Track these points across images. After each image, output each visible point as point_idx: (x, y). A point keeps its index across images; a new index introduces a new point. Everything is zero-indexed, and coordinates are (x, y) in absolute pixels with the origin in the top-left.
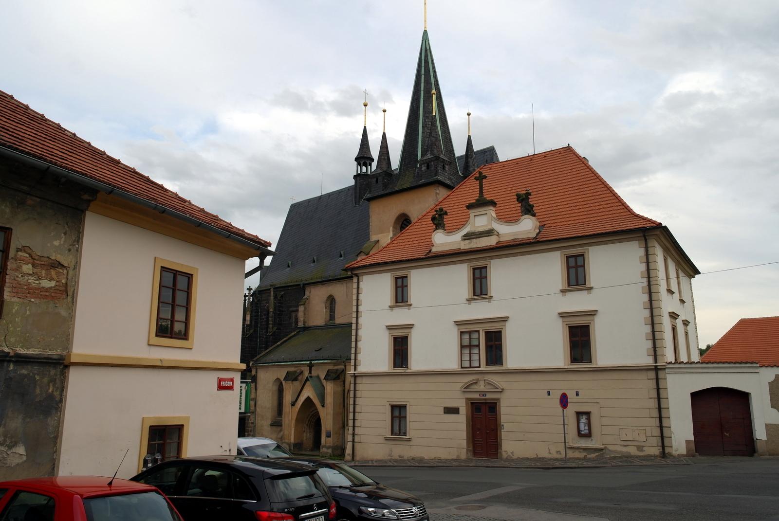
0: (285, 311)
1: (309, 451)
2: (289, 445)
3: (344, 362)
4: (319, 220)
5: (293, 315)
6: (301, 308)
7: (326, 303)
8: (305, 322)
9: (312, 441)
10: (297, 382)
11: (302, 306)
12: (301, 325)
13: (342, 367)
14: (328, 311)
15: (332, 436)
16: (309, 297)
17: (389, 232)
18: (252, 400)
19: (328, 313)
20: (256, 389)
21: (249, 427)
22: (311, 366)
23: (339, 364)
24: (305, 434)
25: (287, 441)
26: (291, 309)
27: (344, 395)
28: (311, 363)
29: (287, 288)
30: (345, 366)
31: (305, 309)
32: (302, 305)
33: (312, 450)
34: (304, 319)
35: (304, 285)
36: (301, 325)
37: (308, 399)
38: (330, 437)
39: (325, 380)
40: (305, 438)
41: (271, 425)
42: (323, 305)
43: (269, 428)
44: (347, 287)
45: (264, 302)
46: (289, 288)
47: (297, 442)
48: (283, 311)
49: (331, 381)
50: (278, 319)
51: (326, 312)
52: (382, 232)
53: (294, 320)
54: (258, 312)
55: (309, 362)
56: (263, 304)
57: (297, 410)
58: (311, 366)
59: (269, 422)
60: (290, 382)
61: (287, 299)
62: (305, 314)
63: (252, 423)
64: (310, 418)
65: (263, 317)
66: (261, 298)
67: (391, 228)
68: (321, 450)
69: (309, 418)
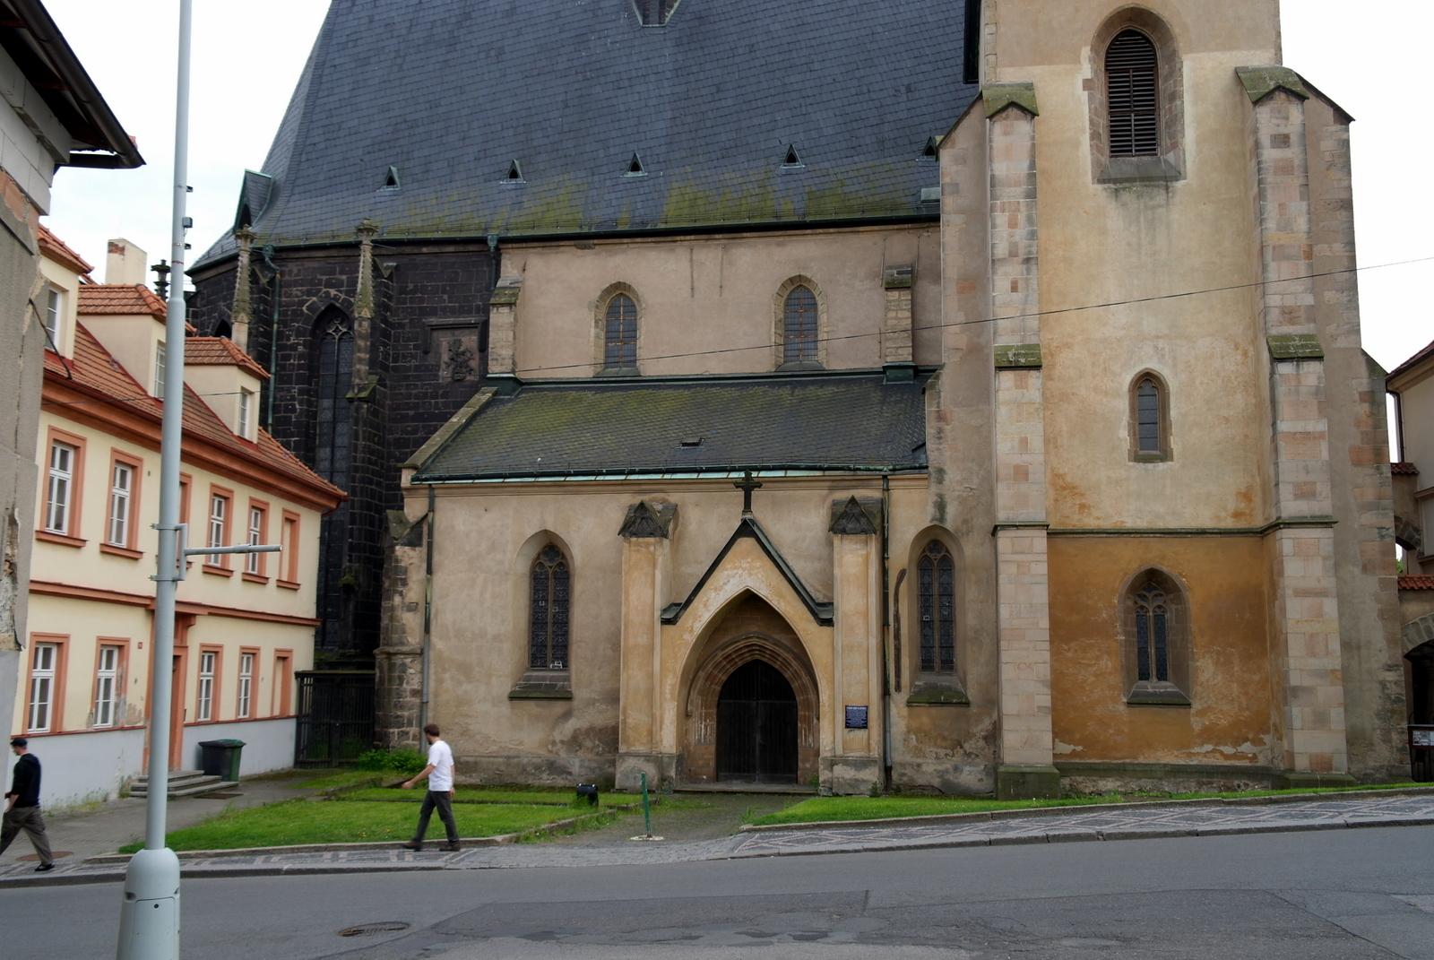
0: (401, 326)
1: (708, 781)
2: (657, 760)
3: (885, 477)
4: (493, 53)
6: (500, 319)
9: (713, 748)
11: (505, 310)
14: (603, 334)
17: (1077, 61)
18: (412, 608)
19: (602, 342)
20: (429, 571)
21: (402, 707)
22: (748, 487)
23: (863, 483)
25: (641, 748)
26: (434, 320)
28: (748, 477)
29: (408, 250)
32: (502, 305)
33: (717, 779)
35: (503, 241)
36: (496, 369)
37: (748, 603)
38: (865, 726)
41: (513, 697)
42: (590, 317)
43: (505, 708)
44: (691, 260)
45: (295, 291)
46: (425, 250)
49: (863, 537)
50: (382, 349)
51: (597, 336)
52: (1046, 59)
53: (445, 357)
54: (270, 324)
55: (742, 475)
56: (290, 296)
58: (748, 487)
59: (506, 687)
60: (652, 540)
61: (411, 286)
63: (415, 693)
65: (293, 340)
66: (282, 274)
67: (1086, 52)
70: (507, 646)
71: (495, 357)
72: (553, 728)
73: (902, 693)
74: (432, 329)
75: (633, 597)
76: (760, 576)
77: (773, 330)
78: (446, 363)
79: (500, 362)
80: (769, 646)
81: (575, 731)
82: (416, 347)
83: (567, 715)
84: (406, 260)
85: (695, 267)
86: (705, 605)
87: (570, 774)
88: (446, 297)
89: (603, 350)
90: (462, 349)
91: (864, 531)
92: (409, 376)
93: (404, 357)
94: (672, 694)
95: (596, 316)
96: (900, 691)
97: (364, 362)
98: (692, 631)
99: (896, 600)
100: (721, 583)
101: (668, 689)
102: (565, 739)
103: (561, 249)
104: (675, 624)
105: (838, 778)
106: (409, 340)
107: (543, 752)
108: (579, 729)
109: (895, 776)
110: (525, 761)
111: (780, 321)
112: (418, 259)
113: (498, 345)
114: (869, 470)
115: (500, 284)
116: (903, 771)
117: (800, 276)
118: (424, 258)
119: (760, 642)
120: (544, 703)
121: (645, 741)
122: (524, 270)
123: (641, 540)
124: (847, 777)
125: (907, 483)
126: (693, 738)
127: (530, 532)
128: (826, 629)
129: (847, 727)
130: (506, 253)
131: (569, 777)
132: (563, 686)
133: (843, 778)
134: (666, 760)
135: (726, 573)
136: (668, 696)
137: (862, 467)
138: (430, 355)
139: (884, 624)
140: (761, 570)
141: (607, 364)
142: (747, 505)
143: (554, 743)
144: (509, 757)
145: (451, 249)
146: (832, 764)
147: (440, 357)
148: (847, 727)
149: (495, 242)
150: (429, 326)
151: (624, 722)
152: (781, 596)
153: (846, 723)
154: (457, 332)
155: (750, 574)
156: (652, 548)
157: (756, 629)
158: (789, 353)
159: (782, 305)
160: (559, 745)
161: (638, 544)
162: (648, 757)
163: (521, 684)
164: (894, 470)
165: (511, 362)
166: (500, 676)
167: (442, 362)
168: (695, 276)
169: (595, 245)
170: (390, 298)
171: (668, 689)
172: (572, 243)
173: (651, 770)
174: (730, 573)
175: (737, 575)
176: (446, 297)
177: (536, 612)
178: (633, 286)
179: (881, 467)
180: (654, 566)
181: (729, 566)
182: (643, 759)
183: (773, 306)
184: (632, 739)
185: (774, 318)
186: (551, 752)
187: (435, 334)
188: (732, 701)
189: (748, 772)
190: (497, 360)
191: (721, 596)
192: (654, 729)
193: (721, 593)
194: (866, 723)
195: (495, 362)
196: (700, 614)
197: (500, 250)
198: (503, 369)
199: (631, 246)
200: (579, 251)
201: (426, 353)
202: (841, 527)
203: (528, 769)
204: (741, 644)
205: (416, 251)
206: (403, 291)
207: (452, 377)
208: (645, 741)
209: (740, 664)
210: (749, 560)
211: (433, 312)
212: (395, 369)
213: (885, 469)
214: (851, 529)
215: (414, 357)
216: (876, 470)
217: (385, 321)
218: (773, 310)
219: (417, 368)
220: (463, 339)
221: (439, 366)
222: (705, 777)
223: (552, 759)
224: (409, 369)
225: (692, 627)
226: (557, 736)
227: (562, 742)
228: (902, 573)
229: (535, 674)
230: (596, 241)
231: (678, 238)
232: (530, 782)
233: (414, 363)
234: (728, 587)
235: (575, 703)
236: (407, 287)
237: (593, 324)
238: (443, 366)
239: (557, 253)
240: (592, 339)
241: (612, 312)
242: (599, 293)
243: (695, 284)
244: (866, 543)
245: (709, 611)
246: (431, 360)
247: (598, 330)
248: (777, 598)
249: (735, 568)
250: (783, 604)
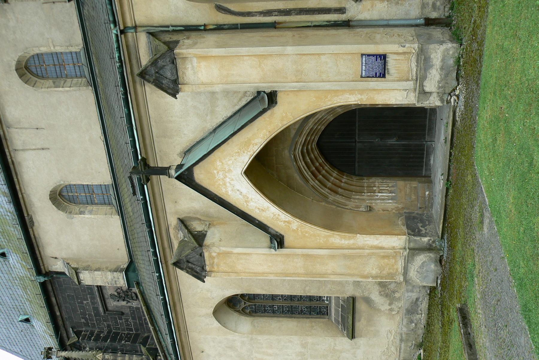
0: (109, 326)
1: (431, 189)
2: (414, 251)
3: (122, 32)
5: (112, 304)
7: (70, 213)
8: (117, 270)
9: (401, 183)
10: (209, 234)
11: (81, 276)
12: (122, 282)
13: (143, 40)
14: (90, 208)
15: (380, 49)
16: (64, 260)
19: (95, 208)
24: (378, 205)
25: (400, 265)
26: (101, 309)
27: (234, 27)
30: (135, 27)
31: (87, 268)
33: (428, 179)
34: (110, 271)
35: (39, 272)
38: (383, 57)
39: (177, 92)
40: (391, 205)
41: (353, 336)
43: (360, 341)
44: (23, 150)
47: (404, 229)
48: (109, 332)
49: (179, 61)
50: (123, 342)
51: (91, 212)
53: (124, 303)
57: (296, 223)
59: (343, 342)
60: (206, 255)
61: (83, 320)
62: (98, 269)
64: (326, 186)
68: (434, 102)
69: (325, 191)
70: (310, 340)
71: (114, 282)
72: (379, 310)
73: (347, 6)
74: (107, 310)
75: (260, 269)
76: (230, 162)
77: (61, 89)
78: (127, 303)
79: (117, 280)
80: (302, 139)
81: (381, 295)
82: (121, 319)
83: (368, 301)
84: (67, 323)
85: (28, 148)
86: (263, 210)
87: (417, 299)
88: (85, 302)
89: (100, 207)
90: (116, 294)
91: (173, 61)
92: (139, 323)
93: (128, 325)
94: (350, 238)
95: (76, 214)
96: (345, 8)
97: (131, 358)
98: (288, 222)
99: (249, 14)
100: (241, 197)
101: (345, 242)
102: (388, 302)
103: (37, 236)
104: (283, 237)
105: (439, 88)
106: (117, 322)
107: (398, 318)
108: (380, 292)
109: (434, 15)
110: (405, 329)
111: (54, 83)
112: (65, 316)
113: (105, 280)
114: (118, 48)
115: (68, 274)
116: (430, 6)
117: (16, 70)
118: (64, 313)
119: (299, 147)
120: (357, 316)
121: (393, 261)
122: (56, 258)
123: (207, 263)
124: (438, 78)
125: (126, 8)
126: (391, 205)
127: (216, 324)
128: (280, 98)
129: (384, 76)
130: (48, 269)
131: (420, 300)
132: (344, 301)
133: (439, 82)
134: (412, 245)
135: (230, 193)
136: (352, 242)
137: (117, 55)
138: (123, 311)
139: (273, 26)
140: (224, 162)
141: (110, 204)
142: (164, 171)
143: (391, 310)
144: (401, 340)
145: (53, 300)
146: (423, 93)
147: (123, 306)
148: (384, 76)
149: (40, 277)
150: (105, 313)
151: (373, 277)
152: (248, 143)
153: (380, 77)
154: (106, 296)
155: (230, 171)
156: (214, 254)
157: (286, 153)
158: (78, 73)
159: (42, 81)
160: (393, 306)
161: (212, 265)
162: (408, 260)
163: (342, 329)
164: (115, 22)
165: (115, 273)
166: (335, 344)
167: (126, 305)
168: (34, 147)
169: (28, 215)
170: (92, 333)
171: (345, 242)
172: (30, 230)
173: (421, 259)
174: (230, 189)
175: (232, 182)
176: (85, 302)
177: (283, 312)
178: (50, 189)
179: (114, 35)
180: (231, 253)
181: (224, 190)
182: (410, 265)
183: (43, 90)
184: (391, 271)
185: (52, 89)
186: (398, 311)
187: (110, 308)
188: (357, 165)
189: (423, 150)
190: (115, 281)
191: (253, 197)
192: (382, 254)
193: (250, 197)
194: (380, 56)
195: (117, 283)
196: (272, 215)
197: (46, 272)
198: (121, 278)
199: (23, 192)
200: (35, 224)
201: (123, 314)
202: (172, 86)
203: (412, 328)
204: (302, 164)
205: (60, 318)
206: (87, 324)
207: (136, 300)
208: (393, 261)
209: (321, 160)
210: (215, 172)
211: (96, 309)
212: (137, 330)
213: (115, 32)
214: (172, 74)
215: (127, 320)
216: (118, 41)
217: (105, 339)
218: (46, 90)
219: (134, 318)
220: (110, 293)
221: (130, 307)
222: (427, 193)
223: (405, 311)
224: (135, 324)
225: (285, 222)
226: (385, 307)
227: (390, 304)
228: (220, 9)
229: (333, 314)
230: (26, 215)
231: (10, 160)
232: (423, 326)
233: (130, 320)
234: (244, 191)
235: (358, 294)
236: (84, 322)
237: (83, 216)
238: (129, 304)
239: (40, 238)
240: (92, 216)
241: (72, 200)
242: (60, 212)
243: (40, 147)
244: (184, 59)
245: (268, 207)
246: (127, 311)
247: (86, 212)
248: (251, 146)
249: (225, 184)
250: (256, 141)
